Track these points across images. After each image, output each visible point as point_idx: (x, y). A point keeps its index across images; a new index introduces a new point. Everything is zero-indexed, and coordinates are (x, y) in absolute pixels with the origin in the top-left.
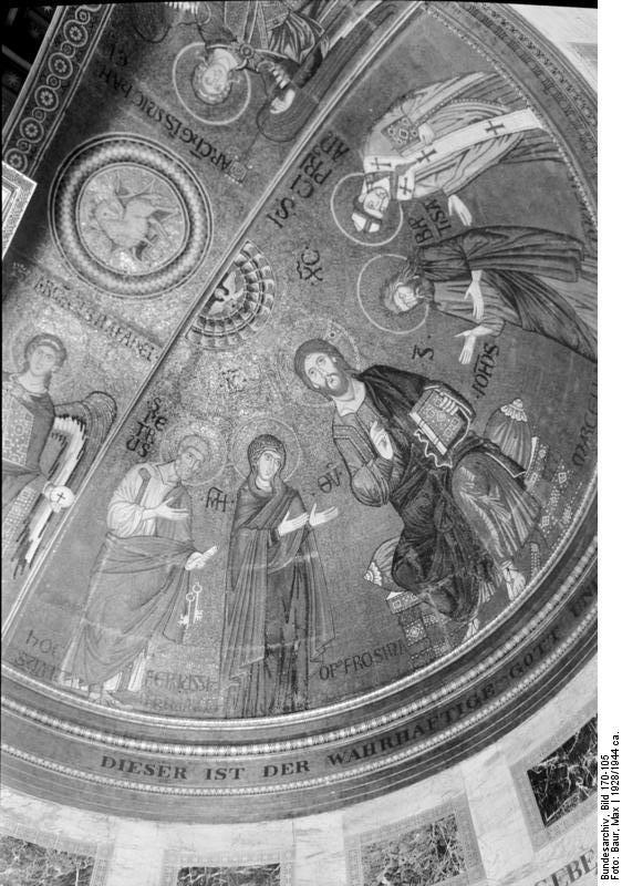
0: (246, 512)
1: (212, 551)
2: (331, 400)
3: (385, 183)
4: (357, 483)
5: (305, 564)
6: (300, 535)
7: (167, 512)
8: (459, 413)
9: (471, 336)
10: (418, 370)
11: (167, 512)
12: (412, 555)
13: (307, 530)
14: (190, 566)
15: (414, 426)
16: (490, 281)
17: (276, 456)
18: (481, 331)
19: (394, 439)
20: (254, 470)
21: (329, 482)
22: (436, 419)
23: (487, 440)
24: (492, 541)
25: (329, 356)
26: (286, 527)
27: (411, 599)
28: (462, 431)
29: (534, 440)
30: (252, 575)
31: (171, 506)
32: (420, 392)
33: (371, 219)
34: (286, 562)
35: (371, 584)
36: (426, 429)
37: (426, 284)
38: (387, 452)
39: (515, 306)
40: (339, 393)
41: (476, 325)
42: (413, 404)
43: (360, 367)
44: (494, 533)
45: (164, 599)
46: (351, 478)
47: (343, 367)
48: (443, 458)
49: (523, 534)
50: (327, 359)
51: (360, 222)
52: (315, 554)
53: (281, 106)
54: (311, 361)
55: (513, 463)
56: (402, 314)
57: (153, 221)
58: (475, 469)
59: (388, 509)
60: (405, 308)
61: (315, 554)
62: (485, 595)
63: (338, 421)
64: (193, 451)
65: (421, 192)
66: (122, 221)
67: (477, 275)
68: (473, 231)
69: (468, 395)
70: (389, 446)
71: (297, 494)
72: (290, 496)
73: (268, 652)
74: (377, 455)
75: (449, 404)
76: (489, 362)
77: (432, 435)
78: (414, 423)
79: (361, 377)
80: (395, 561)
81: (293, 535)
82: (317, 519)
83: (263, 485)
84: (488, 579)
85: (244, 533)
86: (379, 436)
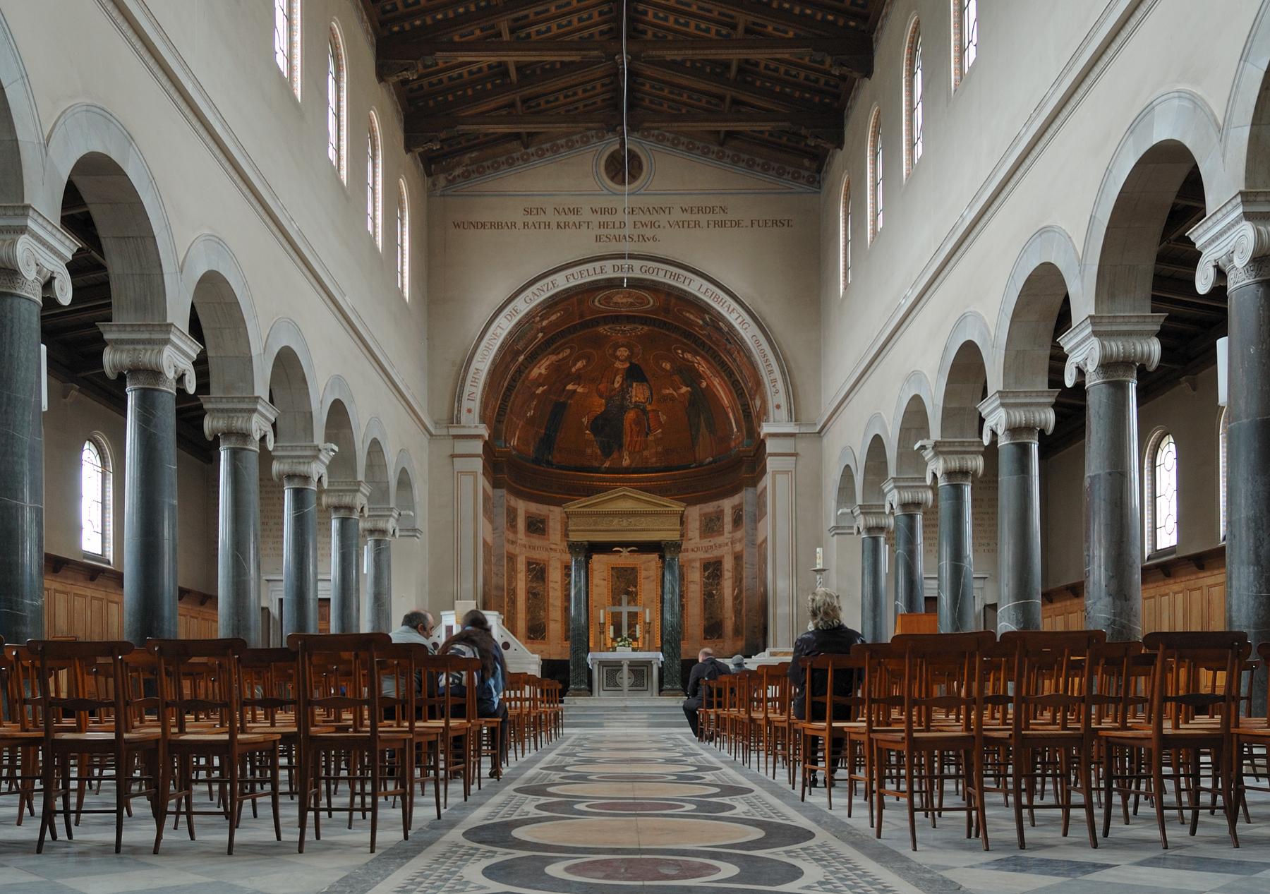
4: (600, 387)
7: (543, 371)
9: (671, 391)
10: (647, 377)
11: (543, 371)
13: (575, 391)
15: (632, 386)
16: (691, 394)
19: (622, 385)
20: (575, 365)
22: (638, 393)
24: (626, 440)
26: (570, 387)
27: (592, 437)
28: (642, 402)
29: (660, 430)
32: (642, 381)
38: (617, 385)
39: (689, 405)
40: (622, 361)
44: (629, 439)
47: (629, 358)
48: (631, 402)
49: (637, 449)
55: (649, 427)
62: (615, 455)
67: (689, 389)
68: (701, 388)
69: (654, 398)
72: (578, 378)
73: (545, 434)
75: (647, 393)
77: (634, 393)
79: (631, 363)
81: (569, 390)
82: (580, 390)
84: (619, 450)
86: (618, 379)
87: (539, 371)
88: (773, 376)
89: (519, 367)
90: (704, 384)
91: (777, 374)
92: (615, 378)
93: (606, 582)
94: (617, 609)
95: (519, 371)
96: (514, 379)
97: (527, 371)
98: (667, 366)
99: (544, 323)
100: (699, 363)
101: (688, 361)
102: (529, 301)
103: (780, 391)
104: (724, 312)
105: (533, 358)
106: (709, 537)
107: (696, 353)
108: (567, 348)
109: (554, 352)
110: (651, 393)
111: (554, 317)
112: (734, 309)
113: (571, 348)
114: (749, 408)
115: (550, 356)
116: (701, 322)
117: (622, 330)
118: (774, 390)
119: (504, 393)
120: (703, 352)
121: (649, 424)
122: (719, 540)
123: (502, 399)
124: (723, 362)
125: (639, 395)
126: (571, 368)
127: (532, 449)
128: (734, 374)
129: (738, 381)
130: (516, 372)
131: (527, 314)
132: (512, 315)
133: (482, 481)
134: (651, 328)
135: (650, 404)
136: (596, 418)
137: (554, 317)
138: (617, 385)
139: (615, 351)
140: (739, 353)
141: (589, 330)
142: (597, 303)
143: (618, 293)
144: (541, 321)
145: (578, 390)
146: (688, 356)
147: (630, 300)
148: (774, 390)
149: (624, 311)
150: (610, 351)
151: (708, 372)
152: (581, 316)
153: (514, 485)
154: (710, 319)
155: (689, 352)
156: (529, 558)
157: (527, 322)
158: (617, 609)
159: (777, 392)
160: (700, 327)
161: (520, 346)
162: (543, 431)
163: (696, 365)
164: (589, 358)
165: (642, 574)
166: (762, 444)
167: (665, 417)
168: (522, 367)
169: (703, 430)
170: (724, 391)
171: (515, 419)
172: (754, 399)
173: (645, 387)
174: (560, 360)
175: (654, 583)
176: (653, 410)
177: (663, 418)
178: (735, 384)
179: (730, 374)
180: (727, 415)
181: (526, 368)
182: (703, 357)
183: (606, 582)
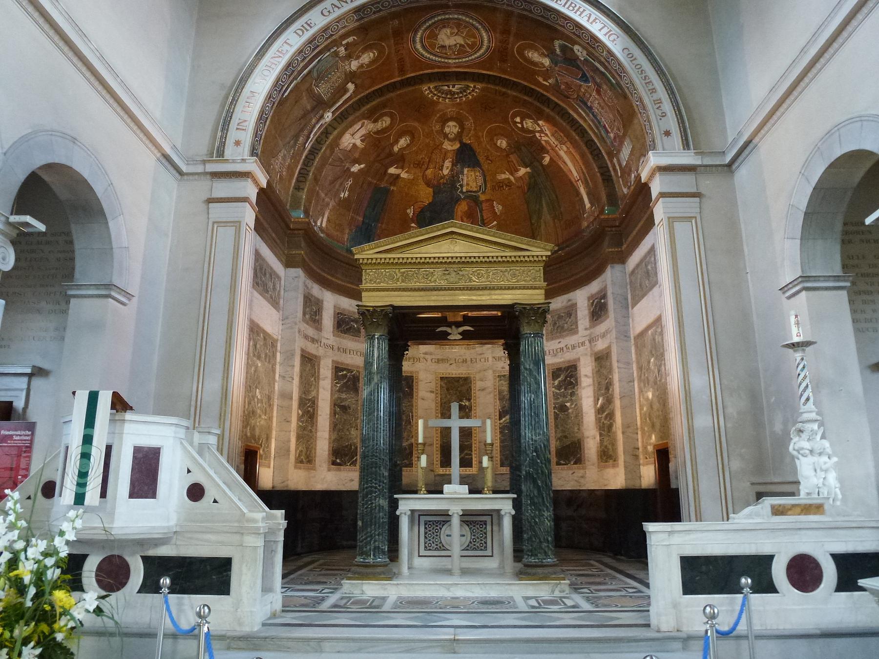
0: (383, 156)
1: (362, 166)
2: (444, 139)
3: (538, 129)
5: (390, 189)
6: (394, 177)
7: (358, 143)
8: (480, 186)
10: (481, 159)
11: (358, 143)
12: (428, 214)
13: (398, 176)
14: (352, 170)
15: (462, 173)
16: (531, 176)
17: (409, 141)
18: (512, 178)
19: (452, 170)
20: (397, 142)
21: (418, 164)
22: (470, 179)
23: (481, 204)
25: (459, 128)
26: (392, 170)
28: (474, 192)
30: (370, 183)
31: (361, 140)
33: (521, 123)
34: (383, 185)
35: (408, 215)
36: (465, 178)
37: (513, 150)
38: (446, 172)
39: (529, 189)
40: (449, 140)
41: (512, 174)
42: (468, 167)
43: (466, 141)
45: (339, 182)
46: (427, 169)
47: (459, 137)
48: (462, 192)
50: (457, 129)
51: (518, 119)
52: (395, 189)
53: (541, 79)
54: (451, 123)
56: (496, 144)
57: (458, 45)
58: (470, 207)
59: (431, 190)
60: (498, 144)
61: (395, 189)
63: (440, 147)
64: (384, 122)
65: (543, 142)
66: (449, 37)
67: (528, 170)
68: (542, 165)
70: (448, 170)
71: (404, 160)
72: (400, 160)
73: (363, 222)
74: (442, 170)
75: (480, 181)
76: (504, 187)
77: (465, 182)
78: (463, 172)
79: (461, 142)
80: (420, 212)
81: (392, 175)
83: (396, 149)
85: (377, 164)
86: (448, 164)
87: (353, 141)
88: (655, 97)
89: (326, 128)
90: (547, 160)
91: (662, 93)
92: (444, 162)
93: (433, 395)
94: (445, 423)
95: (326, 133)
96: (319, 142)
97: (336, 132)
98: (503, 143)
99: (354, 65)
100: (541, 131)
101: (528, 131)
102: (327, 14)
103: (669, 114)
104: (583, 21)
105: (343, 119)
106: (558, 338)
107: (539, 115)
108: (385, 114)
109: (373, 115)
110: (485, 181)
111: (367, 58)
112: (596, 19)
113: (391, 116)
114: (609, 171)
115: (366, 121)
116: (546, 62)
117: (450, 91)
118: (659, 112)
119: (306, 157)
120: (547, 110)
121: (482, 216)
122: (571, 340)
123: (304, 164)
124: (574, 120)
125: (471, 183)
126: (392, 145)
127: (346, 236)
128: (587, 132)
129: (593, 141)
130: (322, 133)
131: (325, 29)
132: (303, 29)
133: (250, 241)
134: (484, 85)
135: (484, 193)
136: (422, 211)
137: (367, 58)
138: (446, 172)
139: (443, 127)
140: (598, 92)
141: (411, 89)
142: (419, 46)
143: (444, 24)
144: (349, 57)
145: (402, 176)
146: (529, 124)
147: (460, 40)
148: (659, 112)
149: (453, 63)
150: (438, 127)
151: (553, 141)
152: (402, 71)
153: (318, 271)
154: (563, 48)
155: (530, 117)
156: (338, 363)
157: (327, 48)
158: (445, 423)
159: (664, 115)
160: (547, 75)
161: (323, 90)
162: (361, 219)
163: (537, 135)
164: (411, 133)
165: (478, 385)
166: (643, 190)
167: (500, 207)
168: (330, 129)
169: (546, 216)
170: (574, 160)
171: (323, 195)
172: (619, 151)
173: (478, 174)
174: (378, 132)
175: (492, 395)
176: (487, 201)
177: (498, 208)
178: (590, 143)
179: (582, 132)
180: (578, 194)
181: (335, 129)
182: (549, 120)
183: (433, 395)
